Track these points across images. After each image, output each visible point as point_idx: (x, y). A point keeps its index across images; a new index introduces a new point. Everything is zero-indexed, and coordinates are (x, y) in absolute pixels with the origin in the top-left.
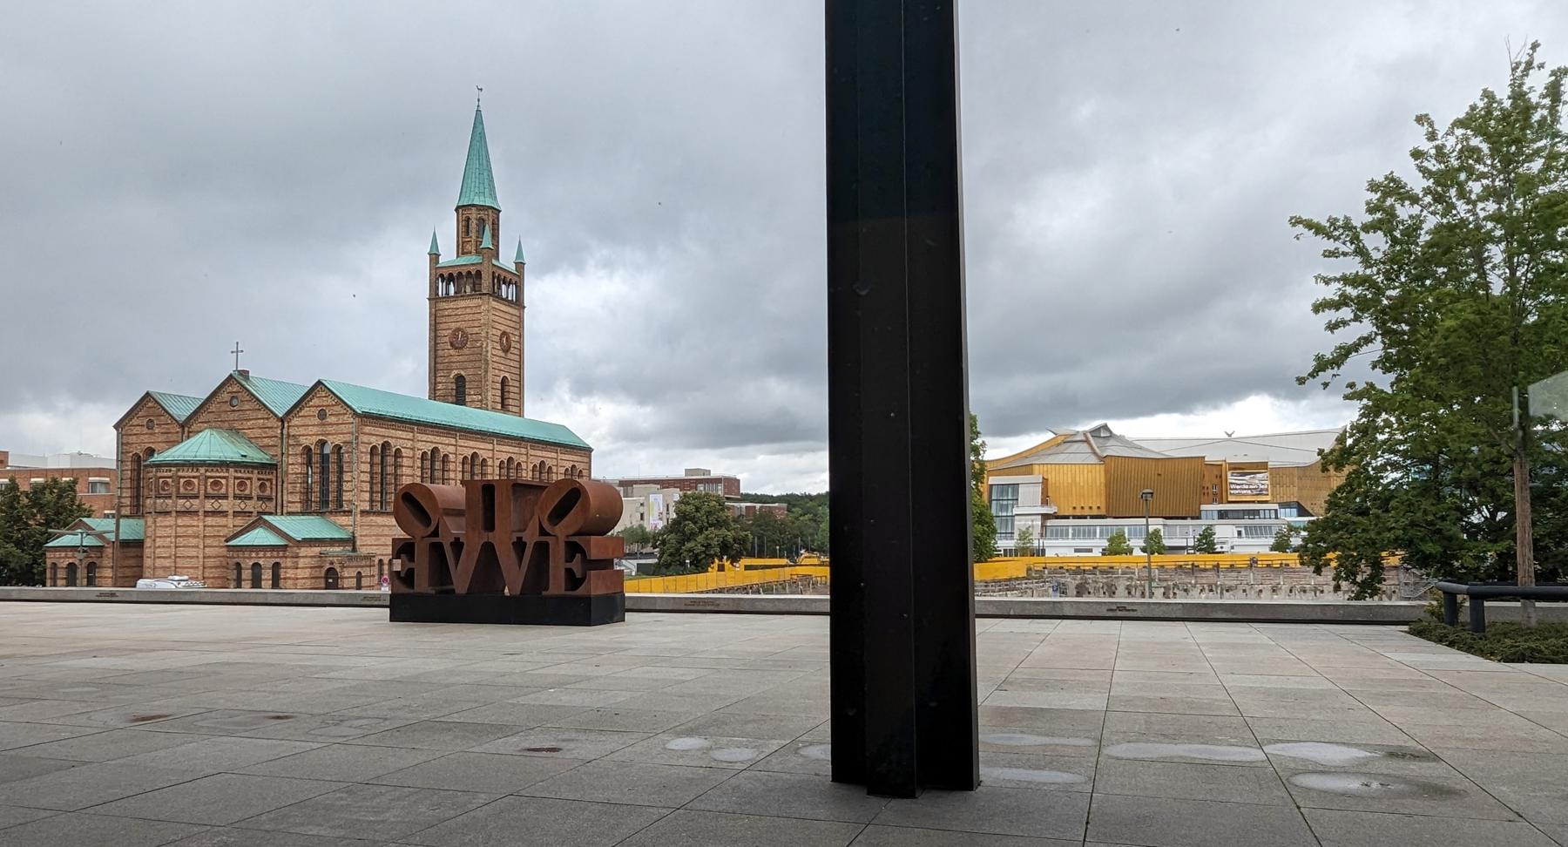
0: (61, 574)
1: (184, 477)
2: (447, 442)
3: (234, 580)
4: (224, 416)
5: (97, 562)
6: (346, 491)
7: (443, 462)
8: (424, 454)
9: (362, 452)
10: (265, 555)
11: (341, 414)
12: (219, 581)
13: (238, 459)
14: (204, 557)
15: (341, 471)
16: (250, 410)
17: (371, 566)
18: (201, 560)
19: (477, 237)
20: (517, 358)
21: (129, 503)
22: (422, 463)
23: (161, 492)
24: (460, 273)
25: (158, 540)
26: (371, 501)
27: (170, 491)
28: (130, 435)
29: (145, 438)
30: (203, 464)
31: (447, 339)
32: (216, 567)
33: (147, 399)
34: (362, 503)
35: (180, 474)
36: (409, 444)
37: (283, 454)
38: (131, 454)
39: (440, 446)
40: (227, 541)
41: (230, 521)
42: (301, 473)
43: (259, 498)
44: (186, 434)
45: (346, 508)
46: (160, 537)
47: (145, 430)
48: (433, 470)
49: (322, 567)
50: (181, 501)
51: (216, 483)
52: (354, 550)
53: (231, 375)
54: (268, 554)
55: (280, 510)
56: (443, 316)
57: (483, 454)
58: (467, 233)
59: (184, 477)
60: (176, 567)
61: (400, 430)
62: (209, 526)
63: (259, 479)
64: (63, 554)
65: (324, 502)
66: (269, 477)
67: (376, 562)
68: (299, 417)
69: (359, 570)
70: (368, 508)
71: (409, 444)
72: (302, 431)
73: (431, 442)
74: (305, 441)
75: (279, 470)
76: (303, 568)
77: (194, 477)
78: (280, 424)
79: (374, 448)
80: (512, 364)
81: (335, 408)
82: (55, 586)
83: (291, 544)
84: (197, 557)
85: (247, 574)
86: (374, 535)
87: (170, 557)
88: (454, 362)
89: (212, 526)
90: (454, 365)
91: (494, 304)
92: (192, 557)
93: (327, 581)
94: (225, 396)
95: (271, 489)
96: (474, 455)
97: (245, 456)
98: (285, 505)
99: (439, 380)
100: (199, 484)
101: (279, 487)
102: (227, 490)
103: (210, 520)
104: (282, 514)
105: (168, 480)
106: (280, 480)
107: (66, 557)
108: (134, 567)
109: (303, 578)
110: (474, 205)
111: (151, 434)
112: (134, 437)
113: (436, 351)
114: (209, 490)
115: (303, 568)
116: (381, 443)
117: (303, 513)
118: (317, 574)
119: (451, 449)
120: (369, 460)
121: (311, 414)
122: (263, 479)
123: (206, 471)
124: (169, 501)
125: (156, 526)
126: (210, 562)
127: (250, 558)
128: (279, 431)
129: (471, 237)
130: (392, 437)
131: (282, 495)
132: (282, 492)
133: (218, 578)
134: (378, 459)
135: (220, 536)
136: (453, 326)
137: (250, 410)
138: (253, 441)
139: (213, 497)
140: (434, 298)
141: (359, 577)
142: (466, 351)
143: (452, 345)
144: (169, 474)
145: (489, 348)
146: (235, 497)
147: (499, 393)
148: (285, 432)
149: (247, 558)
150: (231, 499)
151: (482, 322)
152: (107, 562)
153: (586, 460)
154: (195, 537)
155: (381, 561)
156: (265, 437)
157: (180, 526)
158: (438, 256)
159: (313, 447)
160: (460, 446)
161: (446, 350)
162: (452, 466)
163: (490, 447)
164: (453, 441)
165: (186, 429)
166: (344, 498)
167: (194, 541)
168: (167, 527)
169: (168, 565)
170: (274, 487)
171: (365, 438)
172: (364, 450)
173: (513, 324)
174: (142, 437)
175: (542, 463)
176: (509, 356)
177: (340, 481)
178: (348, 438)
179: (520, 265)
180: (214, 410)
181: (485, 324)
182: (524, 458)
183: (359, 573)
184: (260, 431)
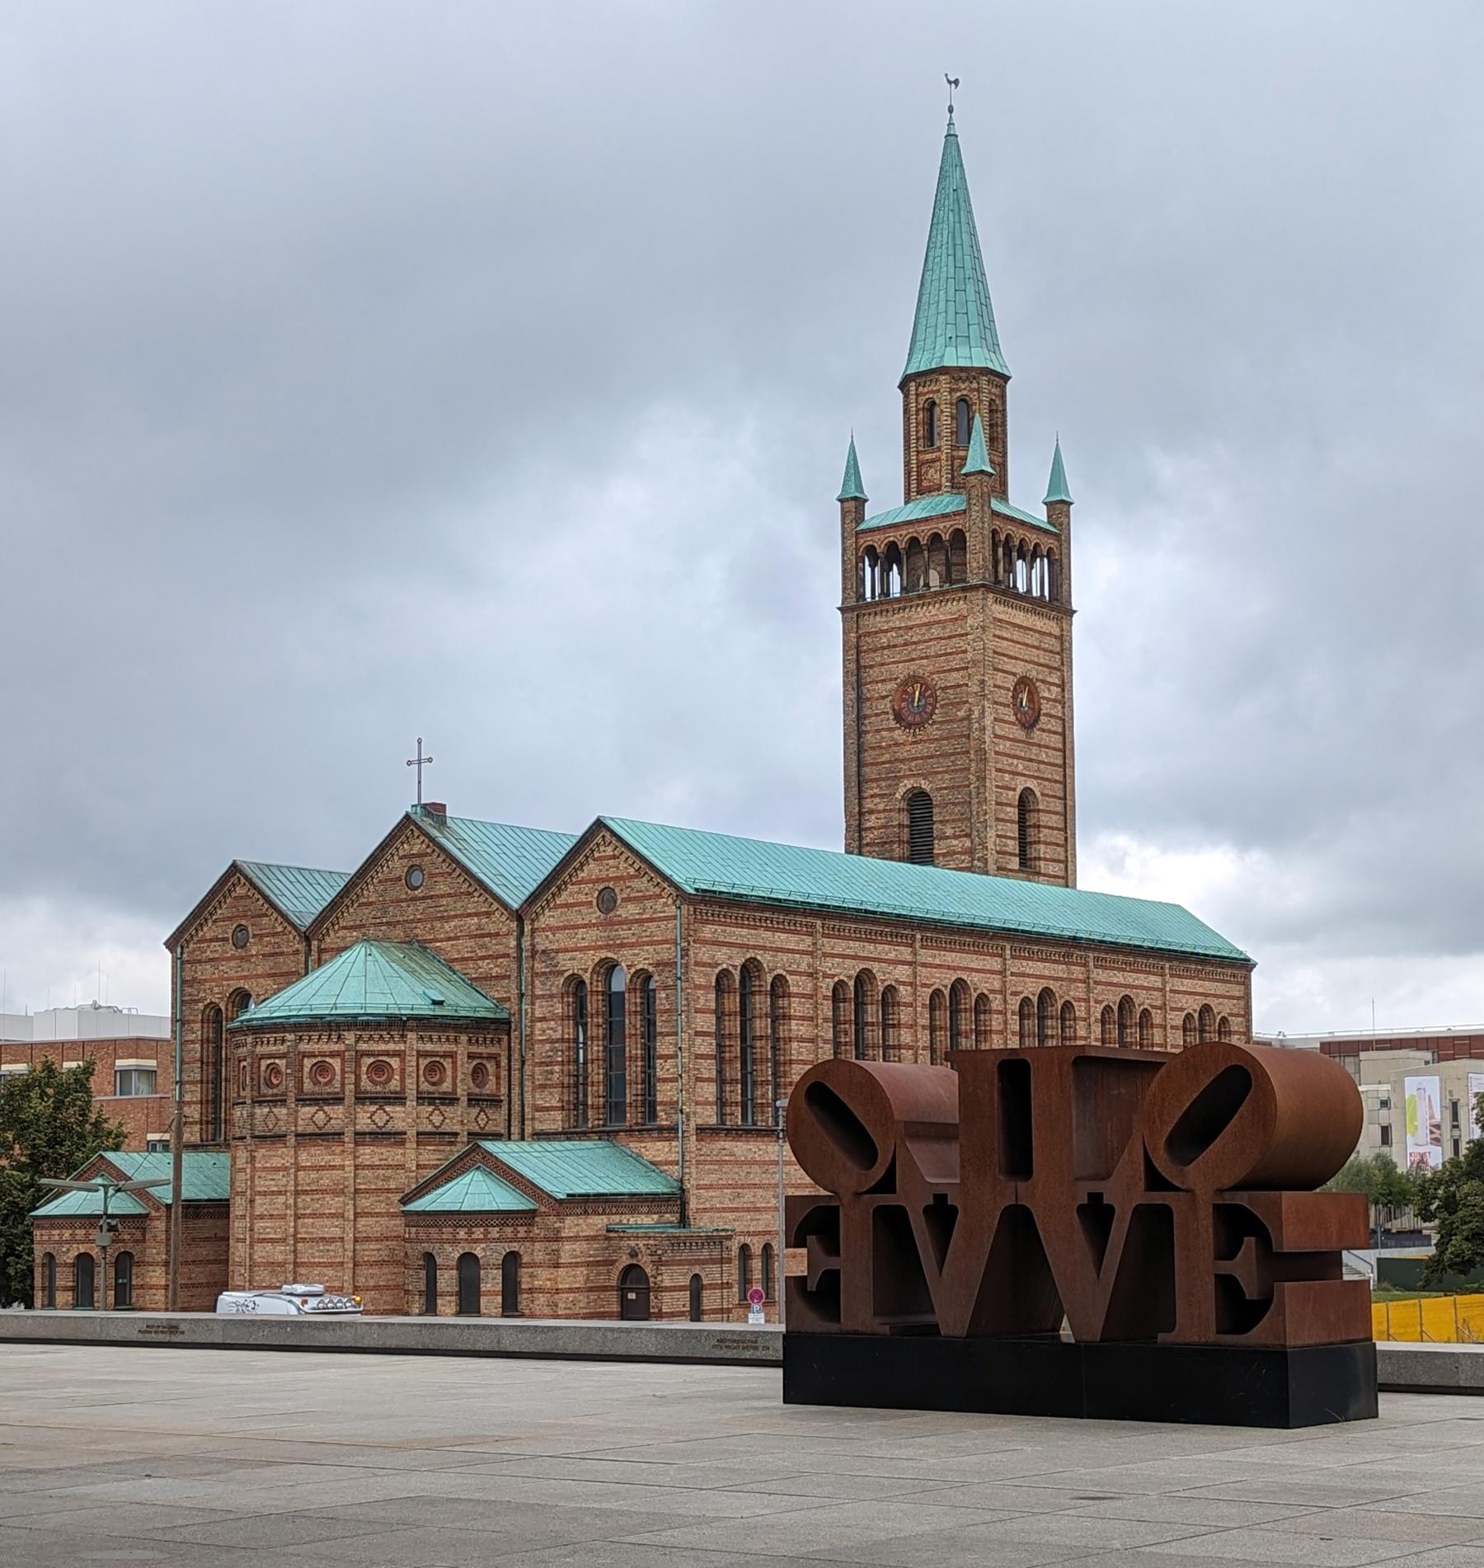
0: (64, 1278)
1: (312, 1055)
2: (892, 956)
3: (421, 1293)
5: (135, 1250)
6: (665, 1080)
7: (885, 1004)
8: (839, 986)
9: (699, 987)
10: (486, 1233)
11: (650, 898)
12: (387, 1296)
13: (425, 1009)
14: (356, 1240)
15: (650, 1034)
17: (721, 1261)
18: (349, 1246)
19: (954, 448)
20: (1055, 741)
21: (197, 1116)
22: (835, 1009)
23: (264, 1090)
24: (914, 541)
25: (259, 1200)
26: (721, 1102)
27: (282, 1088)
28: (200, 962)
30: (353, 1023)
31: (884, 705)
32: (381, 1263)
34: (699, 1109)
35: (304, 1047)
36: (804, 963)
37: (521, 996)
38: (201, 1006)
39: (875, 967)
40: (405, 1201)
41: (409, 1155)
42: (562, 1040)
43: (473, 1100)
44: (314, 955)
45: (663, 1120)
46: (265, 1194)
47: (230, 950)
48: (860, 1024)
49: (613, 1263)
50: (306, 1111)
51: (379, 1068)
52: (683, 1221)
53: (407, 817)
54: (494, 1232)
55: (518, 1129)
57: (980, 983)
58: (930, 438)
59: (312, 1055)
60: (296, 1264)
61: (784, 931)
62: (364, 1167)
63: (471, 1056)
64: (67, 1234)
65: (615, 1107)
66: (493, 1050)
67: (735, 1252)
68: (556, 907)
69: (697, 1270)
70: (713, 1121)
71: (804, 963)
72: (562, 940)
73: (855, 957)
74: (570, 964)
75: (514, 1034)
76: (571, 1265)
77: (332, 1055)
78: (514, 925)
79: (724, 975)
80: (1043, 757)
81: (635, 884)
82: (51, 1304)
83: (543, 1209)
84: (342, 1239)
85: (447, 1280)
86: (729, 1186)
87: (284, 1240)
88: (902, 761)
89: (372, 1167)
91: (999, 610)
92: (332, 1240)
93: (623, 1300)
94: (396, 866)
95: (498, 1078)
96: (959, 987)
97: (440, 1003)
98: (528, 1116)
99: (869, 804)
100: (343, 1072)
101: (516, 1074)
102: (403, 1080)
103: (367, 1154)
104: (523, 1139)
105: (277, 1061)
106: (516, 1056)
107: (73, 1240)
108: (209, 1262)
109: (570, 1290)
110: (943, 370)
111: (242, 958)
114: (366, 1084)
115: (571, 1265)
116: (738, 962)
117: (567, 1135)
118: (602, 1281)
119: (902, 973)
120: (713, 1005)
121: (583, 898)
122: (480, 1056)
123: (359, 1039)
124: (281, 1112)
125: (254, 1169)
126: (370, 1251)
127: (455, 1241)
128: (513, 943)
129: (939, 449)
130: (764, 948)
131: (522, 1094)
132: (522, 1085)
133: (387, 1287)
134: (733, 1003)
135: (388, 1190)
136: (902, 671)
137: (450, 895)
138: (457, 967)
139: (373, 1100)
140: (854, 608)
141: (696, 1288)
142: (932, 731)
143: (898, 717)
144: (283, 1048)
145: (988, 721)
146: (421, 1099)
147: (1013, 830)
148: (526, 943)
149: (448, 1241)
150: (411, 1103)
151: (969, 656)
152: (155, 1252)
153: (1237, 990)
154: (336, 1193)
155: (744, 1248)
156: (482, 958)
157: (304, 1168)
158: (860, 502)
159: (586, 977)
160: (924, 965)
161: (885, 731)
162: (905, 1015)
163: (995, 964)
164: (905, 953)
165: (315, 943)
166: (659, 1098)
167: (334, 1203)
168: (277, 1170)
169: (280, 1258)
170: (504, 1073)
171: (704, 953)
172: (703, 981)
173: (1043, 658)
175: (1125, 1003)
176: (1037, 736)
177: (649, 1057)
178: (666, 953)
179: (1059, 509)
181: (975, 662)
182: (1078, 991)
183: (696, 1277)
184: (471, 943)
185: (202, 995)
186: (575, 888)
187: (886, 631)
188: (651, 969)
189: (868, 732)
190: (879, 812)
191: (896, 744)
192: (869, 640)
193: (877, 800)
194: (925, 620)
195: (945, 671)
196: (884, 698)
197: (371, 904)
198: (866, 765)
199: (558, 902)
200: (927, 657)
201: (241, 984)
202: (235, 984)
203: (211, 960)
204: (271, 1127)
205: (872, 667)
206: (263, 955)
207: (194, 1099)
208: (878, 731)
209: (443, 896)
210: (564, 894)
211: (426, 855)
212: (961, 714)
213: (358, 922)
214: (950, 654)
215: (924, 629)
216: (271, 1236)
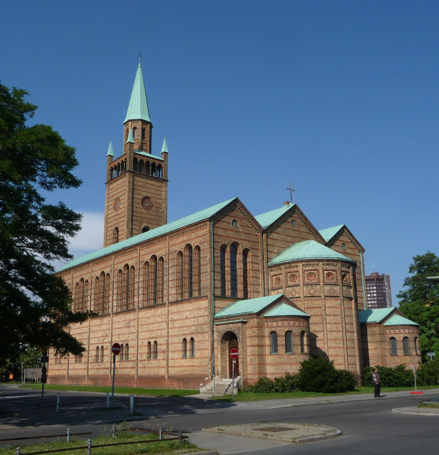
28: (219, 228)
29: (232, 234)
38: (220, 244)
88: (144, 218)
90: (144, 220)
111: (237, 232)
113: (133, 207)
136: (145, 194)
137: (305, 232)
187: (141, 182)
190: (136, 229)
191: (142, 213)
195: (156, 198)
196: (139, 199)
201: (236, 240)
202: (234, 240)
203: (224, 229)
206: (245, 233)
208: (137, 208)
211: (297, 218)
212: (160, 211)
214: (158, 194)
215: (151, 185)
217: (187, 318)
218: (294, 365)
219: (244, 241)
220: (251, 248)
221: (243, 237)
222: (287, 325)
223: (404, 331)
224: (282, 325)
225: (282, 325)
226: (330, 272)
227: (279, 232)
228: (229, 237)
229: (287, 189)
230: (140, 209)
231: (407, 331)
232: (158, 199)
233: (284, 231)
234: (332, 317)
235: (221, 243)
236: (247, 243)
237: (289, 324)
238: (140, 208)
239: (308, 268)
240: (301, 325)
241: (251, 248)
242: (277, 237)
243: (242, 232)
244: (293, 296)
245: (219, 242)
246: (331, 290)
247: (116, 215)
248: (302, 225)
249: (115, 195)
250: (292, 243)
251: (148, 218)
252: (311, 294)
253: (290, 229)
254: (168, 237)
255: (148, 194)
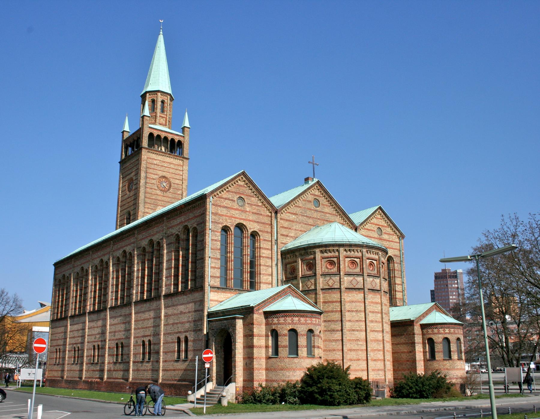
4: (309, 213)
16: (329, 213)
28: (220, 206)
29: (236, 213)
33: (240, 178)
56: (152, 164)
88: (159, 200)
111: (242, 211)
112: (224, 209)
113: (146, 187)
136: (161, 173)
137: (329, 213)
142: (168, 194)
174: (233, 212)
180: (300, 205)
185: (221, 220)
186: (370, 225)
187: (156, 160)
188: (393, 256)
189: (147, 188)
192: (150, 160)
193: (150, 210)
194: (169, 161)
196: (154, 179)
197: (300, 207)
198: (147, 198)
199: (365, 227)
200: (169, 172)
201: (242, 222)
202: (238, 221)
203: (226, 207)
204: (374, 286)
205: (150, 168)
206: (253, 213)
207: (217, 266)
208: (151, 189)
209: (327, 213)
210: (367, 226)
213: (295, 212)
215: (168, 164)
216: (377, 329)
217: (181, 313)
218: (298, 371)
219: (251, 223)
220: (260, 231)
221: (251, 218)
222: (290, 322)
223: (444, 331)
224: (284, 322)
225: (284, 322)
226: (353, 259)
227: (297, 213)
228: (232, 217)
229: (309, 162)
230: (155, 191)
231: (447, 331)
232: (176, 179)
233: (303, 212)
234: (354, 314)
235: (222, 223)
236: (256, 224)
237: (293, 320)
238: (155, 189)
239: (326, 255)
240: (308, 322)
241: (260, 231)
242: (295, 218)
243: (249, 212)
244: (309, 288)
245: (219, 223)
246: (354, 281)
247: (129, 197)
248: (327, 206)
249: (128, 175)
250: (313, 226)
251: (164, 201)
252: (329, 285)
253: (310, 209)
254: (165, 218)
255: (164, 174)
